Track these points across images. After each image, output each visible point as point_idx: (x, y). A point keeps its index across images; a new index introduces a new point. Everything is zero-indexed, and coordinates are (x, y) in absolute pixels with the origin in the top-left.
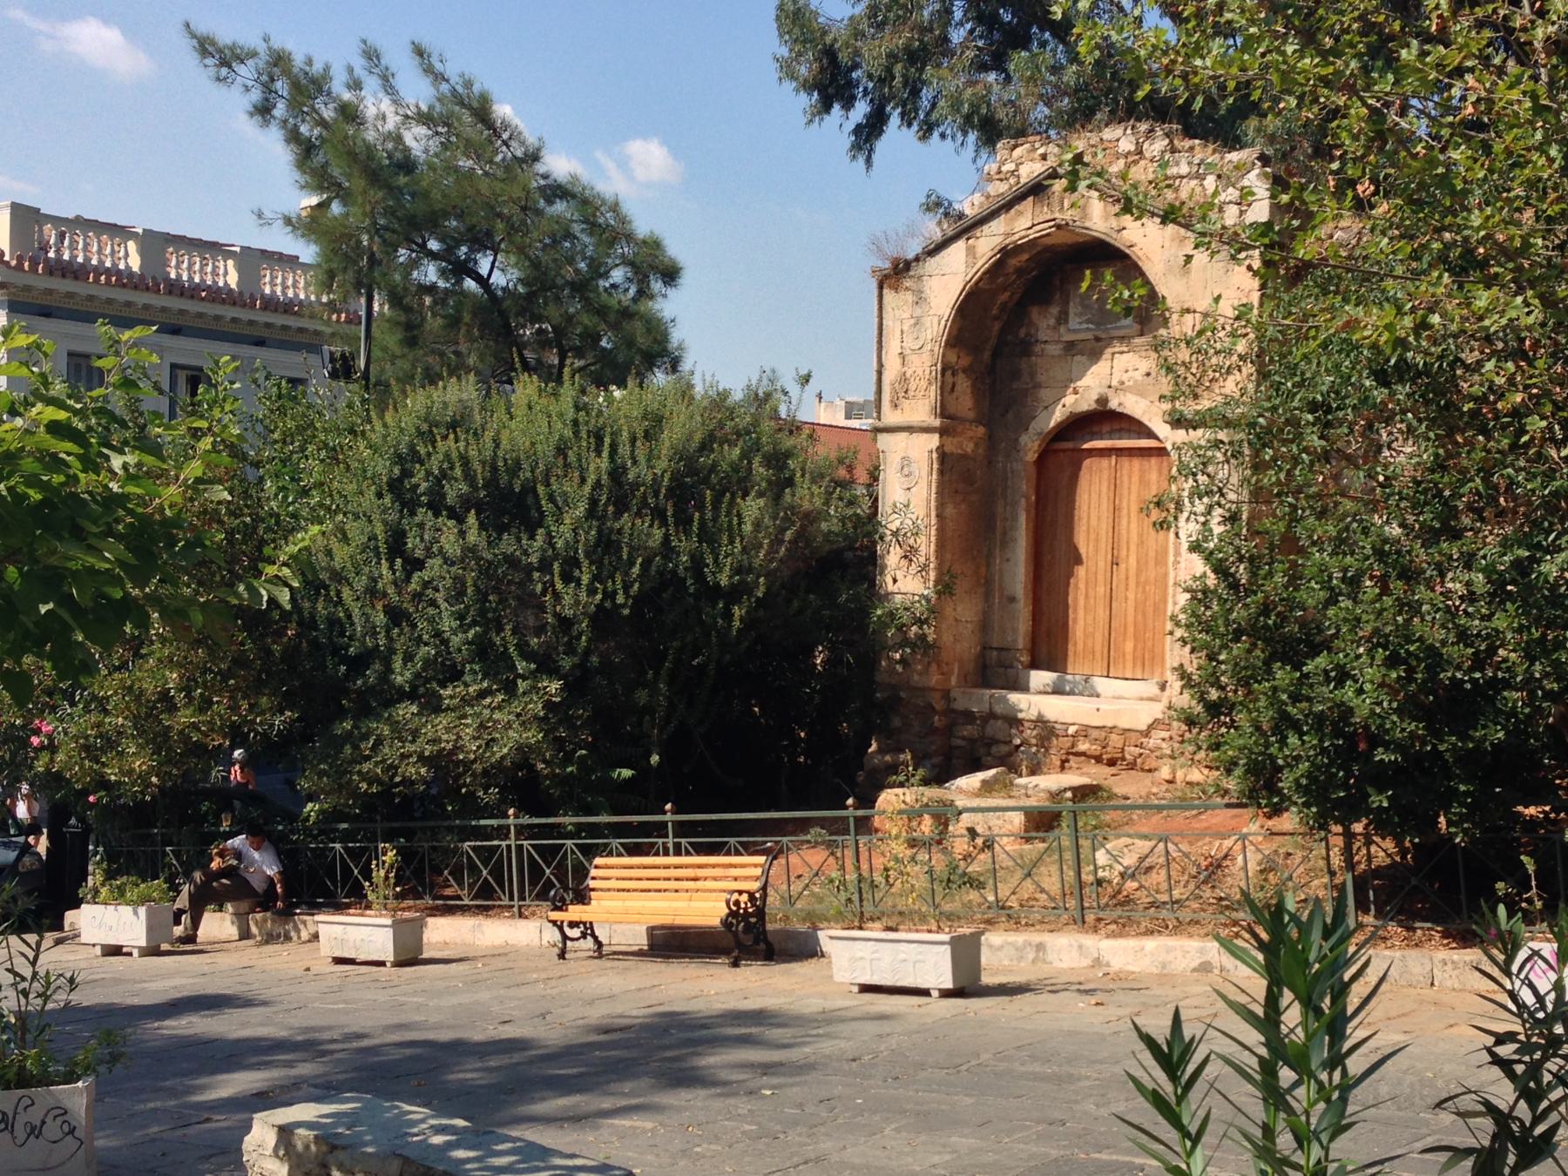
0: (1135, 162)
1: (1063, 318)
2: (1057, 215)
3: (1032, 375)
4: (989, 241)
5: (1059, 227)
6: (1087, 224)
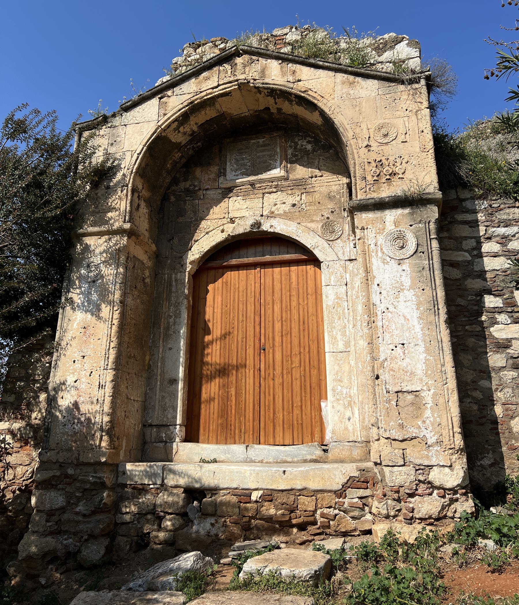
1: (222, 173)
3: (195, 212)
4: (178, 100)
5: (240, 85)
6: (267, 80)
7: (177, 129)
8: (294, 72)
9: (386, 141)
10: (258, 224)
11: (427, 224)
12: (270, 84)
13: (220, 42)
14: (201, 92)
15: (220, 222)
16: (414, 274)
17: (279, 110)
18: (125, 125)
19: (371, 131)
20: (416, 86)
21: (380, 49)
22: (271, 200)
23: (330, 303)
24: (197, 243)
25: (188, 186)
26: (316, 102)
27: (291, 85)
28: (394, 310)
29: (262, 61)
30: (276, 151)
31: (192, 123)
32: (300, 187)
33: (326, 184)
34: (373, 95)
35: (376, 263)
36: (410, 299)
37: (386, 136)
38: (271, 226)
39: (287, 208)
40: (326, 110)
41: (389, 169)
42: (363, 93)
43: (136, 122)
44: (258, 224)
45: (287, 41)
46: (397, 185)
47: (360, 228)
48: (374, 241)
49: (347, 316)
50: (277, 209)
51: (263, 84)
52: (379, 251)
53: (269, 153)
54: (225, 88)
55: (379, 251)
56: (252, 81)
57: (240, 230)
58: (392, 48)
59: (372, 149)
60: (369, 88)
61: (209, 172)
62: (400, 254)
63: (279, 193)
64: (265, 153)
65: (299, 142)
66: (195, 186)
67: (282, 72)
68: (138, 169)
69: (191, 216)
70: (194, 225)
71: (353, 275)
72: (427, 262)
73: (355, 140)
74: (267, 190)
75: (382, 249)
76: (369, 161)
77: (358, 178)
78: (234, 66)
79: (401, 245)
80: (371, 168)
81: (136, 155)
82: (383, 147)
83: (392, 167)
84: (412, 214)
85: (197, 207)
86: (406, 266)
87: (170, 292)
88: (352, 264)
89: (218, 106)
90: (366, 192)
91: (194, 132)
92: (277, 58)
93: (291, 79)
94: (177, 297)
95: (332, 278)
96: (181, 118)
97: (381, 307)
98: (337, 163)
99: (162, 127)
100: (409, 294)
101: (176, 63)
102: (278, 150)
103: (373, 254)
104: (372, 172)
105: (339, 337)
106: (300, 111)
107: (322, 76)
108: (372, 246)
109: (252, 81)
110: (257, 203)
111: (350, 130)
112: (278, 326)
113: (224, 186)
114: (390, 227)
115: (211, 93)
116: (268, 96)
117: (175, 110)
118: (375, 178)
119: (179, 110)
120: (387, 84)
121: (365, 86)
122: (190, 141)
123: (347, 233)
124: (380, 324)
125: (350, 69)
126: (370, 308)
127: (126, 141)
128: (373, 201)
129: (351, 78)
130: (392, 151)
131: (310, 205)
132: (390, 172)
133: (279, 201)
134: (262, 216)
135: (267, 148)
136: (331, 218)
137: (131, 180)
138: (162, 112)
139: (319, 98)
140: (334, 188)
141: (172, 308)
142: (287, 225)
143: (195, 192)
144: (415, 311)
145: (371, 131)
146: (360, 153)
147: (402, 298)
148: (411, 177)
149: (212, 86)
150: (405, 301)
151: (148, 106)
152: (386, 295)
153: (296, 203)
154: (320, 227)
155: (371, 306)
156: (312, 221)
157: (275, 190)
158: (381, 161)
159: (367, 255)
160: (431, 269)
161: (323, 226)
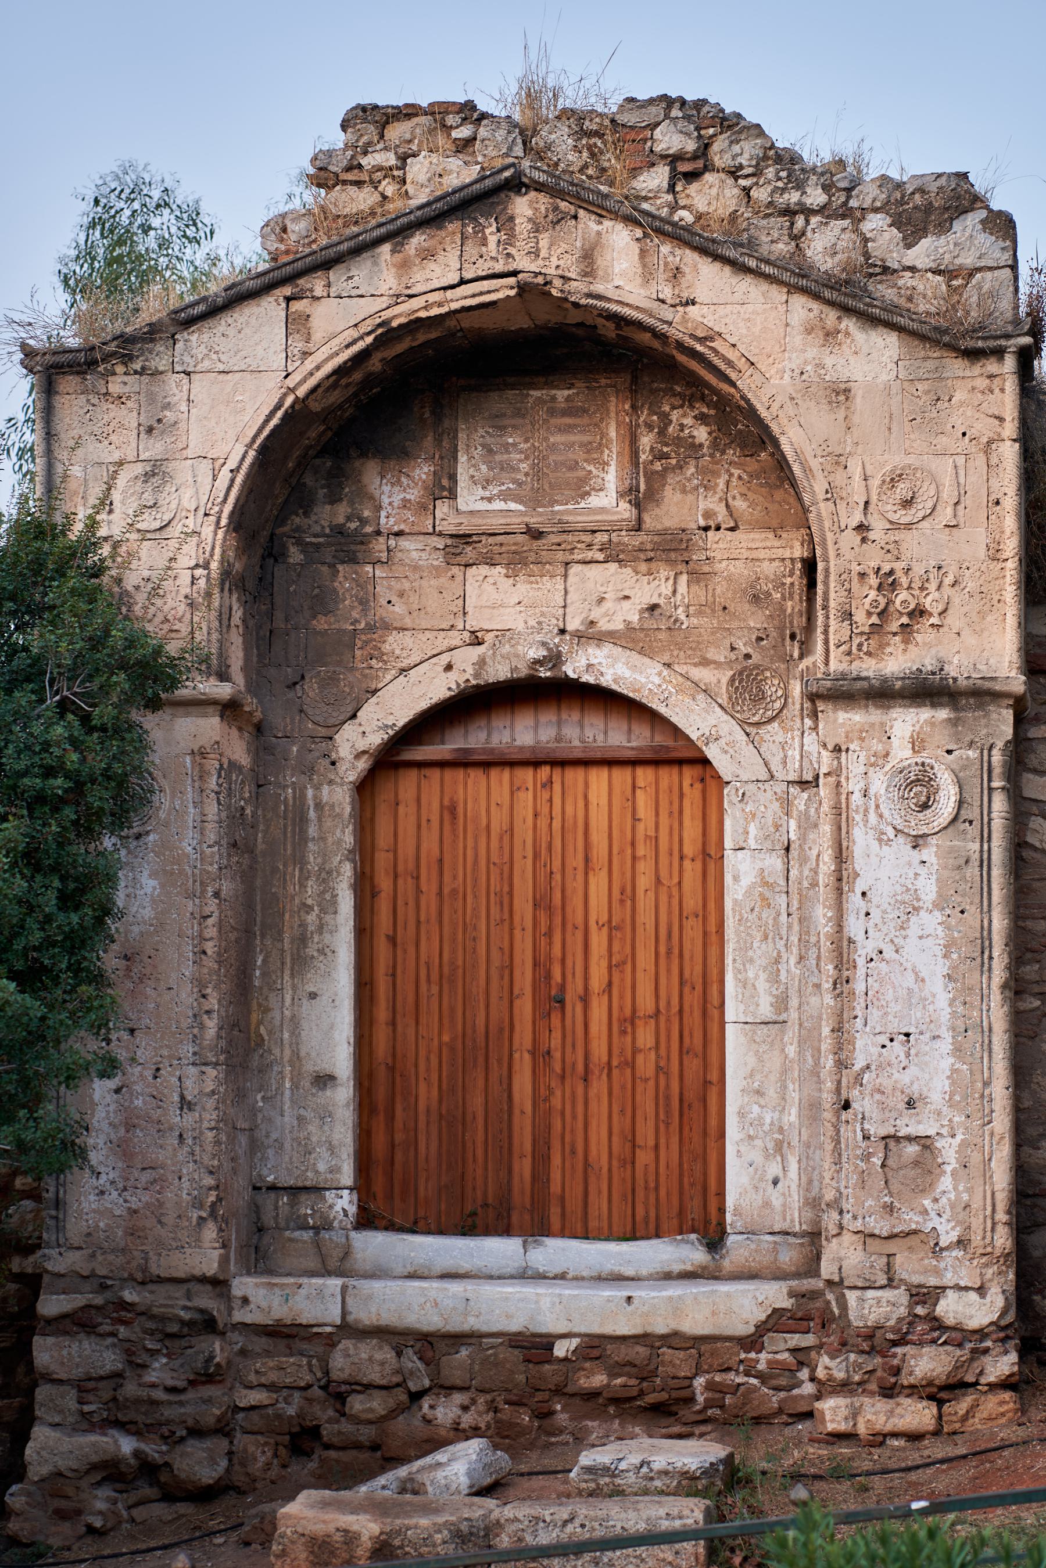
0: (692, 176)
1: (444, 488)
2: (523, 263)
3: (364, 603)
6: (599, 288)
7: (334, 386)
8: (676, 274)
10: (555, 659)
11: (986, 752)
12: (609, 300)
14: (411, 296)
15: (443, 641)
16: (946, 873)
18: (188, 374)
19: (874, 483)
22: (590, 585)
24: (374, 700)
25: (341, 520)
27: (667, 314)
28: (895, 956)
29: (589, 224)
30: (604, 435)
32: (673, 555)
34: (884, 377)
35: (861, 840)
36: (932, 931)
37: (907, 503)
41: (910, 598)
43: (221, 367)
45: (658, 148)
46: (925, 644)
47: (830, 747)
48: (862, 785)
49: (784, 932)
50: (606, 614)
51: (589, 295)
52: (872, 810)
53: (586, 438)
54: (481, 294)
55: (872, 810)
56: (557, 283)
57: (499, 672)
58: (944, 227)
59: (872, 535)
60: (875, 355)
61: (404, 479)
63: (613, 566)
64: (572, 438)
65: (675, 415)
66: (363, 522)
67: (644, 266)
68: (232, 513)
69: (355, 614)
70: (366, 643)
72: (976, 846)
73: (830, 504)
74: (577, 557)
75: (877, 807)
77: (832, 612)
78: (507, 224)
79: (923, 799)
81: (225, 476)
82: (898, 536)
83: (916, 592)
84: (954, 723)
85: (370, 588)
86: (928, 853)
87: (303, 839)
88: (805, 795)
90: (849, 653)
92: (630, 220)
93: (667, 293)
94: (325, 855)
95: (753, 829)
97: (865, 948)
98: (779, 495)
99: (301, 392)
100: (930, 921)
102: (613, 434)
103: (858, 818)
104: (868, 600)
105: (762, 985)
107: (752, 295)
108: (857, 798)
109: (557, 283)
110: (549, 589)
111: (819, 475)
112: (598, 941)
113: (452, 530)
114: (901, 753)
115: (440, 305)
117: (335, 344)
118: (875, 619)
119: (347, 346)
121: (865, 350)
122: (355, 395)
124: (859, 987)
126: (842, 949)
127: (193, 425)
128: (865, 684)
130: (921, 549)
131: (700, 613)
132: (912, 606)
133: (615, 592)
134: (563, 631)
135: (578, 421)
136: (756, 658)
137: (218, 551)
139: (741, 364)
141: (312, 887)
142: (634, 668)
143: (364, 541)
144: (941, 961)
145: (874, 483)
146: (841, 544)
147: (913, 930)
150: (921, 938)
151: (253, 321)
152: (878, 921)
153: (661, 601)
154: (725, 680)
155: (845, 943)
156: (705, 662)
157: (600, 556)
158: (891, 572)
159: (844, 816)
160: (985, 863)
161: (732, 680)
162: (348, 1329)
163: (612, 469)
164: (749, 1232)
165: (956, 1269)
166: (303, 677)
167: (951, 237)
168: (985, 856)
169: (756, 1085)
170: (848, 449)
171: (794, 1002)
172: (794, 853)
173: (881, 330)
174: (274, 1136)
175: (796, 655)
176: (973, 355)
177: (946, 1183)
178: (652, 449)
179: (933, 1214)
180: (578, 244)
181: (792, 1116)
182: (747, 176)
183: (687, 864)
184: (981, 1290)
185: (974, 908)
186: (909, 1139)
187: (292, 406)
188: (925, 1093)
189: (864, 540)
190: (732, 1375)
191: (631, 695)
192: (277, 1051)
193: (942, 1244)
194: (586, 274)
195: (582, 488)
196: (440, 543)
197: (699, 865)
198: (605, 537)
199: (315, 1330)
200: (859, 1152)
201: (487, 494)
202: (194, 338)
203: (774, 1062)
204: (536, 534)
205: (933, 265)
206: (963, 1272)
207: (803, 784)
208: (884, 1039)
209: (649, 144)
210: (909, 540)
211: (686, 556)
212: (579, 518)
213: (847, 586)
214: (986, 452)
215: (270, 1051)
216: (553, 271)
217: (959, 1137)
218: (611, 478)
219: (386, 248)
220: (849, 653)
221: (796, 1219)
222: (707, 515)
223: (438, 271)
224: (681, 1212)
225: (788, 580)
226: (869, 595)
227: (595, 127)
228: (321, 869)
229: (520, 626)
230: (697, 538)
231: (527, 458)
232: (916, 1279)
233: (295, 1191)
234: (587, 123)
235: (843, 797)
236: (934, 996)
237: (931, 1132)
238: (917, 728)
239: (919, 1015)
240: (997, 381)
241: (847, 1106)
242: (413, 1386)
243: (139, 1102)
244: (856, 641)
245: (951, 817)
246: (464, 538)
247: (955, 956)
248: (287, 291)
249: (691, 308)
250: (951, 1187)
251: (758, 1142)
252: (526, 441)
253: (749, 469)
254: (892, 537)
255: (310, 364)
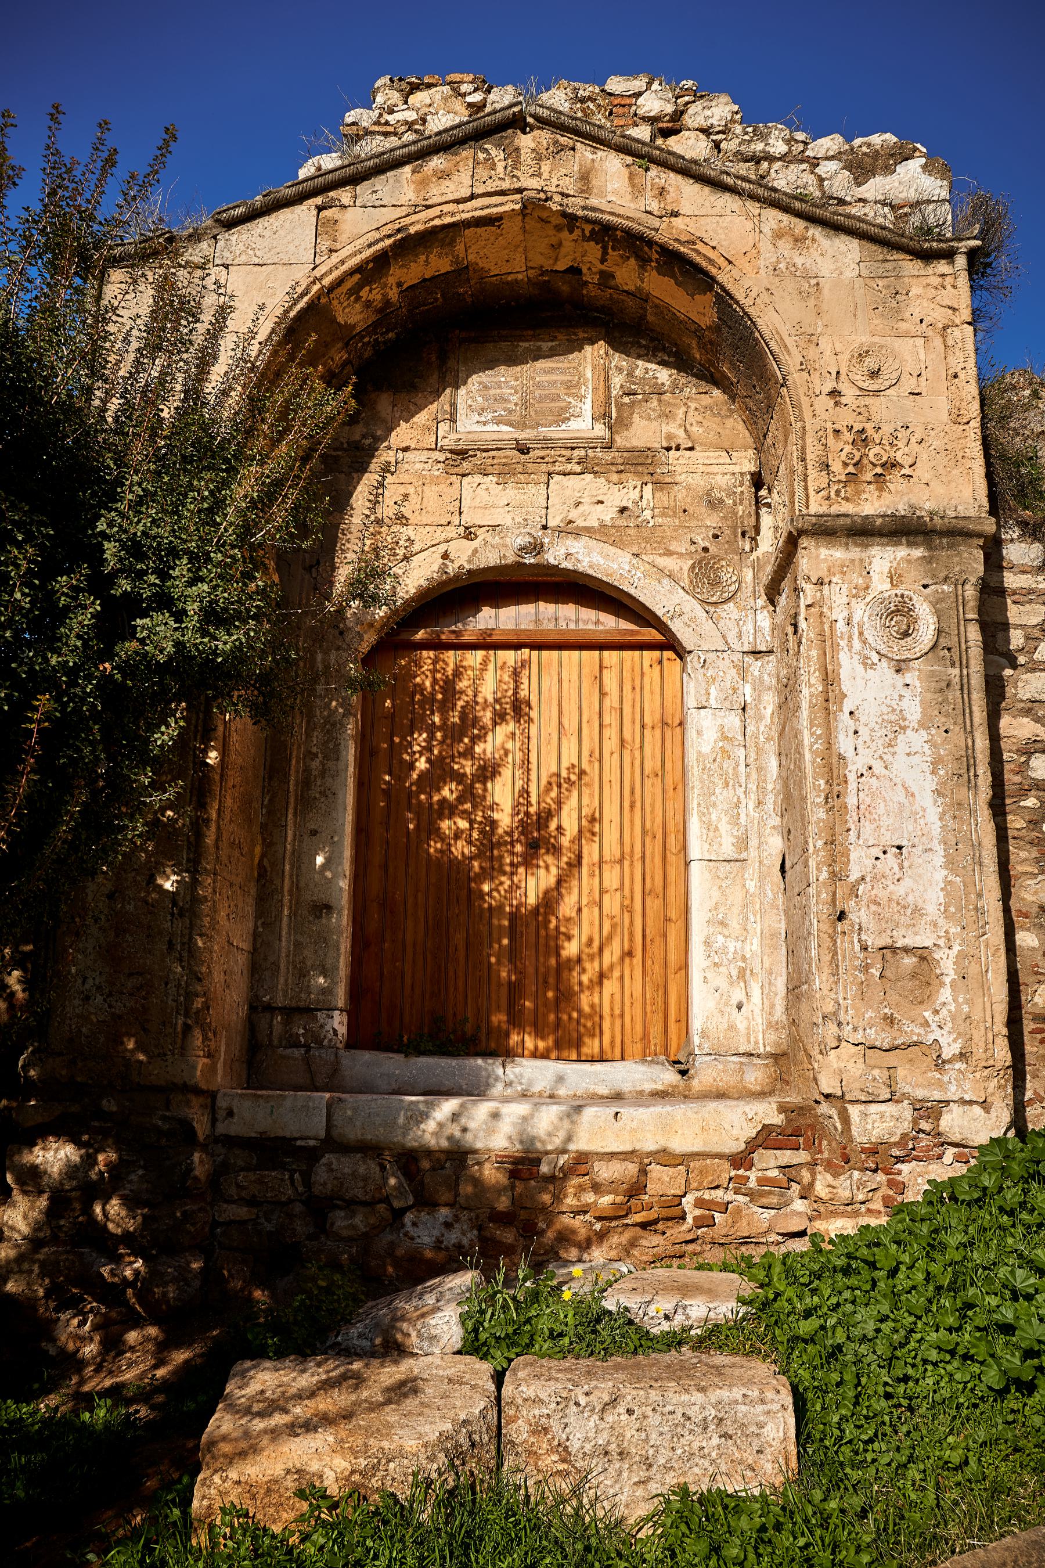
4: (365, 220)
6: (594, 202)
7: (355, 291)
8: (662, 192)
9: (875, 387)
10: (537, 548)
12: (603, 212)
13: (470, 88)
15: (440, 534)
16: (929, 696)
17: (606, 277)
18: (227, 266)
19: (844, 358)
20: (942, 267)
21: (862, 168)
22: (568, 492)
23: (706, 749)
25: (357, 437)
26: (714, 271)
27: (656, 223)
28: (884, 772)
29: (585, 153)
31: (391, 280)
32: (640, 469)
33: (702, 469)
35: (848, 665)
37: (874, 374)
38: (568, 555)
39: (607, 514)
40: (739, 295)
41: (882, 452)
42: (825, 268)
43: (257, 261)
44: (537, 548)
46: (897, 492)
47: (814, 580)
48: (845, 614)
49: (743, 781)
50: (582, 514)
51: (584, 208)
53: (566, 378)
56: (557, 198)
57: (490, 559)
58: (889, 170)
59: (844, 400)
61: (411, 406)
62: (899, 650)
63: (589, 477)
67: (633, 186)
71: (759, 688)
72: (957, 671)
73: (805, 374)
74: (558, 468)
75: (861, 634)
76: (837, 427)
78: (513, 154)
79: (904, 627)
80: (841, 445)
82: (868, 401)
83: (888, 448)
88: (759, 663)
89: (460, 248)
90: (828, 498)
91: (387, 303)
93: (654, 206)
95: (713, 691)
96: (371, 265)
97: (855, 765)
99: (326, 281)
100: (917, 739)
101: (354, 124)
102: (589, 375)
103: (842, 643)
105: (724, 827)
106: (661, 288)
108: (841, 626)
110: (535, 493)
114: (880, 585)
115: (453, 214)
116: (589, 240)
118: (851, 469)
119: (370, 246)
120: (880, 252)
121: (830, 253)
122: (375, 325)
123: (751, 589)
124: (851, 800)
125: (797, 205)
128: (848, 521)
129: (799, 225)
131: (663, 515)
132: (885, 459)
134: (545, 527)
136: (713, 550)
138: (325, 244)
139: (721, 261)
140: (722, 481)
141: (317, 736)
144: (929, 777)
146: (816, 406)
147: (901, 748)
148: (926, 476)
149: (457, 196)
150: (908, 755)
152: (867, 738)
153: (630, 505)
154: (686, 568)
155: (835, 760)
156: (669, 553)
157: (578, 469)
160: (965, 686)
161: (693, 567)
162: (333, 1143)
163: (589, 401)
164: (716, 1054)
165: (957, 1084)
166: (318, 563)
167: (894, 177)
168: (965, 680)
169: (720, 916)
170: (819, 330)
171: (753, 843)
172: (750, 712)
173: (844, 237)
174: (271, 959)
175: (747, 548)
176: (927, 256)
177: (945, 994)
178: (622, 386)
179: (934, 1026)
180: (576, 168)
181: (753, 946)
182: (718, 133)
183: (647, 732)
184: (985, 1105)
185: (957, 728)
186: (907, 950)
187: (318, 296)
188: (920, 904)
189: (837, 404)
190: (719, 1193)
191: (604, 579)
192: (278, 882)
193: (946, 1056)
194: (582, 191)
195: (562, 416)
196: (442, 457)
197: (658, 732)
198: (583, 453)
199: (299, 1143)
200: (857, 963)
201: (483, 419)
202: (234, 238)
203: (737, 897)
204: (524, 450)
205: (881, 197)
206: (967, 1085)
207: (756, 653)
208: (877, 852)
209: (634, 108)
210: (879, 407)
211: (651, 469)
212: (561, 436)
213: (824, 441)
214: (943, 336)
215: (272, 882)
216: (554, 189)
217: (956, 948)
218: (587, 408)
219: (408, 169)
220: (828, 498)
221: (764, 1041)
222: (669, 437)
223: (452, 187)
224: (645, 1037)
225: (740, 489)
226: (841, 450)
227: (587, 94)
228: (326, 722)
229: (508, 522)
230: (662, 456)
231: (516, 392)
232: (920, 1093)
233: (291, 1012)
234: (581, 92)
235: (826, 627)
236: (924, 810)
237: (928, 943)
238: (895, 565)
239: (910, 828)
240: (949, 280)
241: (842, 916)
242: (397, 1204)
243: (130, 908)
244: (834, 488)
245: (930, 645)
246: (462, 454)
247: (941, 772)
248: (319, 200)
249: (673, 219)
250: (950, 998)
251: (722, 969)
252: (516, 379)
253: (704, 403)
254: (862, 401)
255: (335, 258)
